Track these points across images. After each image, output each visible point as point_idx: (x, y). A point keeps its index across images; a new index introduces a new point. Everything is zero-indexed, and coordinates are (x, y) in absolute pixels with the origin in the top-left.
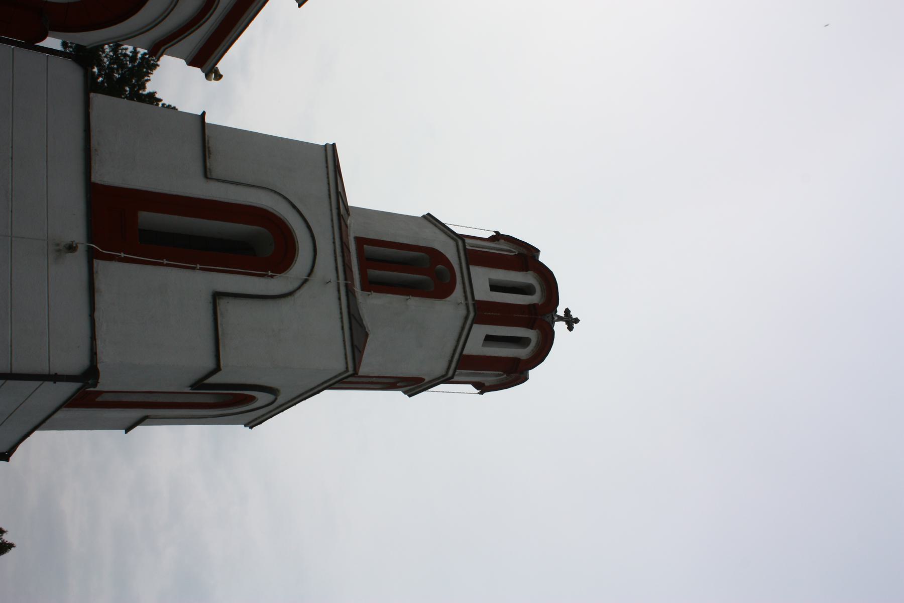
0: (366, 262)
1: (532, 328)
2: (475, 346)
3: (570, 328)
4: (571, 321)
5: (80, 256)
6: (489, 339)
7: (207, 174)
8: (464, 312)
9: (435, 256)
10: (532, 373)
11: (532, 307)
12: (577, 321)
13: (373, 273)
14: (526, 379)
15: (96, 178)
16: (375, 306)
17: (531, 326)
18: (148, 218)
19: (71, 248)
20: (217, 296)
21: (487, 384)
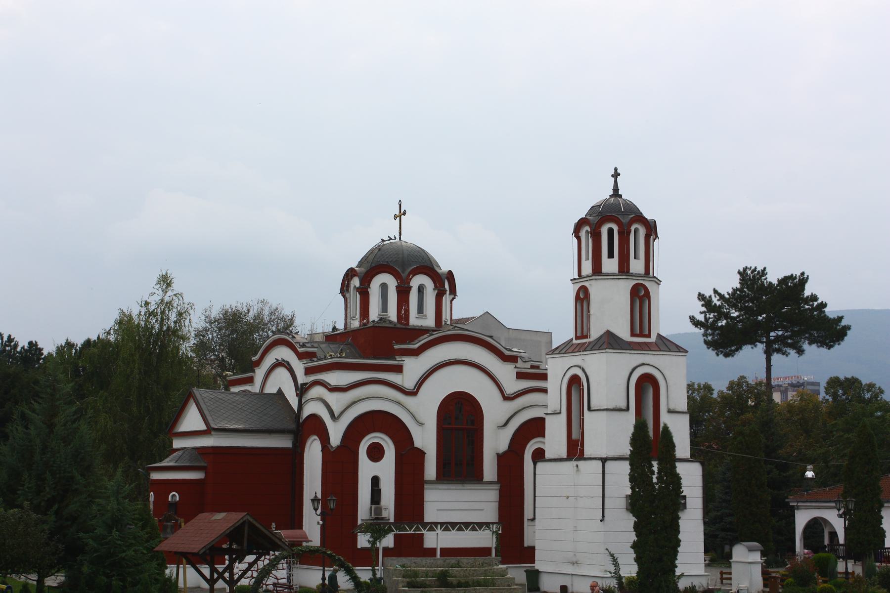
4: (616, 175)
5: (581, 464)
7: (560, 413)
15: (564, 454)
18: (575, 436)
19: (577, 466)
20: (589, 409)
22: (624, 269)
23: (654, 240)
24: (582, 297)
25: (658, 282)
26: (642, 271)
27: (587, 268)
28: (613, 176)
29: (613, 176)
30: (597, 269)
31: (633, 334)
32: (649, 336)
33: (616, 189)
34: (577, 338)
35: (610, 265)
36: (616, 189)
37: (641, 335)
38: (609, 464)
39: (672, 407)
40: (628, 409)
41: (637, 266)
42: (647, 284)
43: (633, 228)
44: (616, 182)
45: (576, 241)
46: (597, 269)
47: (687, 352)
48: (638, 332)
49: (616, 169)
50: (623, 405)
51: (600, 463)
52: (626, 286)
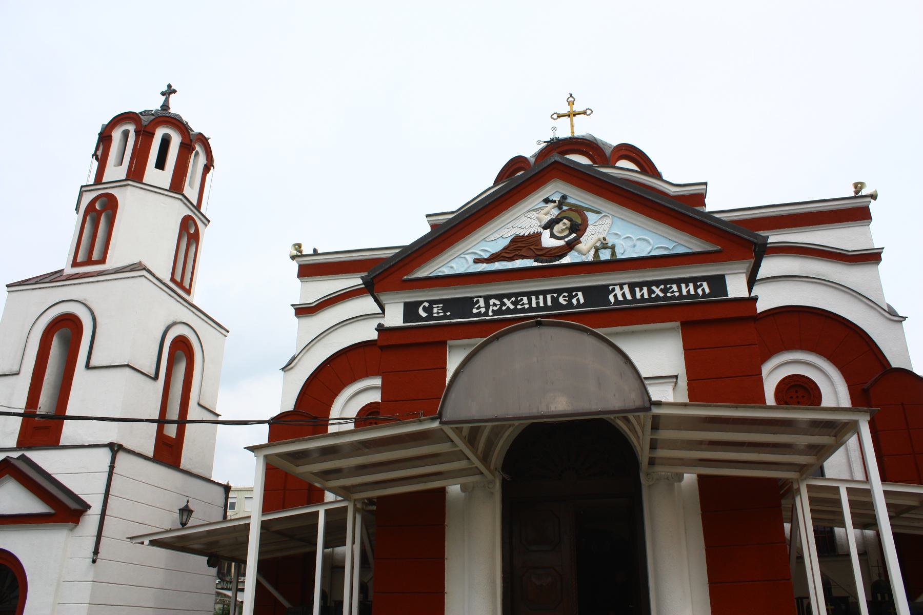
0: (89, 262)
1: (153, 134)
2: (164, 178)
3: (175, 91)
6: (160, 165)
8: (129, 187)
9: (90, 207)
10: (196, 127)
11: (137, 133)
12: (169, 86)
13: (95, 256)
14: (200, 134)
16: (117, 257)
17: (152, 135)
20: (88, 366)
21: (205, 162)
22: (177, 186)
24: (100, 211)
27: (115, 172)
28: (163, 94)
29: (163, 94)
30: (136, 174)
31: (173, 279)
32: (188, 292)
33: (165, 107)
34: (75, 264)
36: (165, 107)
37: (180, 285)
38: (121, 457)
40: (156, 378)
41: (191, 192)
44: (167, 100)
46: (136, 174)
48: (178, 279)
49: (169, 86)
51: (106, 454)
52: (176, 211)
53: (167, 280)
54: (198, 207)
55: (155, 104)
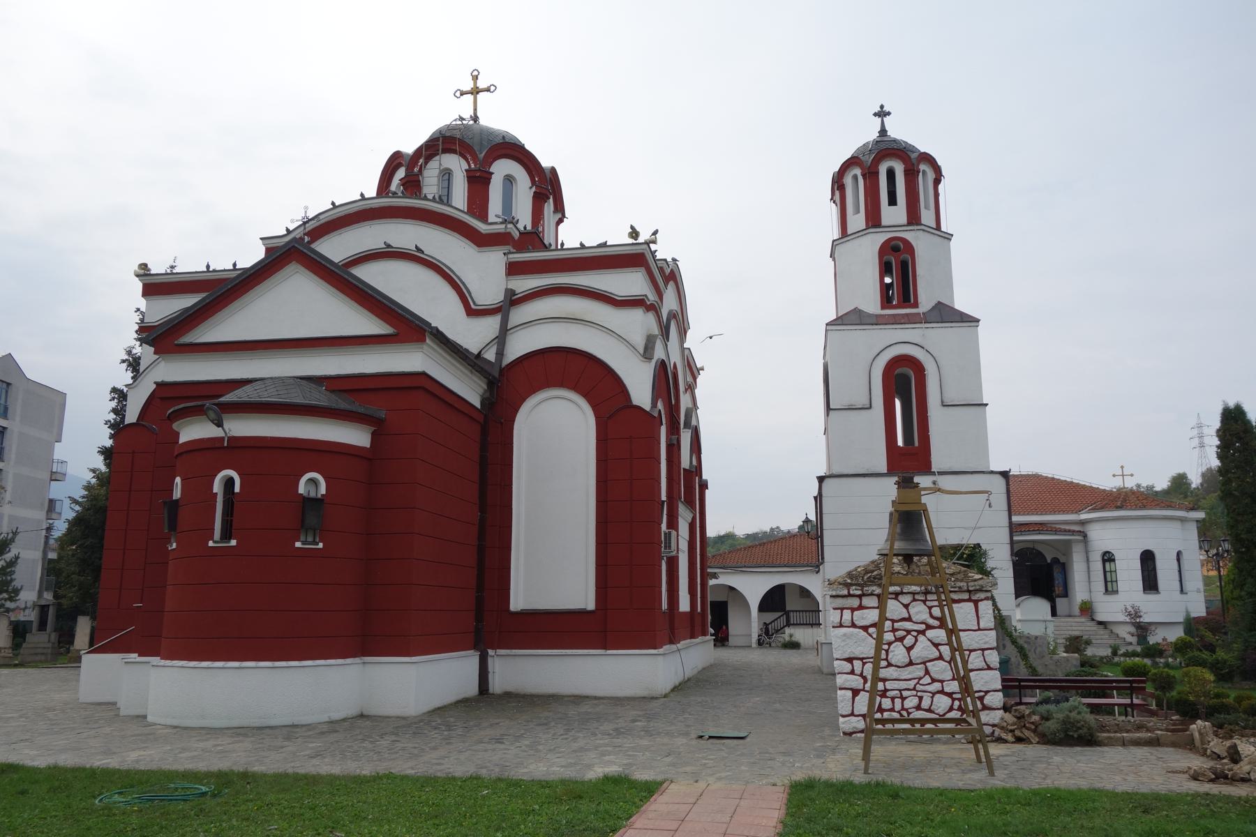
4: (882, 114)
23: (937, 181)
25: (948, 237)
26: (903, 219)
32: (916, 305)
33: (883, 132)
35: (857, 221)
36: (883, 132)
39: (951, 397)
41: (894, 215)
42: (908, 236)
43: (883, 169)
45: (834, 210)
47: (978, 321)
49: (882, 107)
50: (862, 400)
52: (871, 244)
53: (879, 311)
54: (914, 217)
55: (873, 135)
